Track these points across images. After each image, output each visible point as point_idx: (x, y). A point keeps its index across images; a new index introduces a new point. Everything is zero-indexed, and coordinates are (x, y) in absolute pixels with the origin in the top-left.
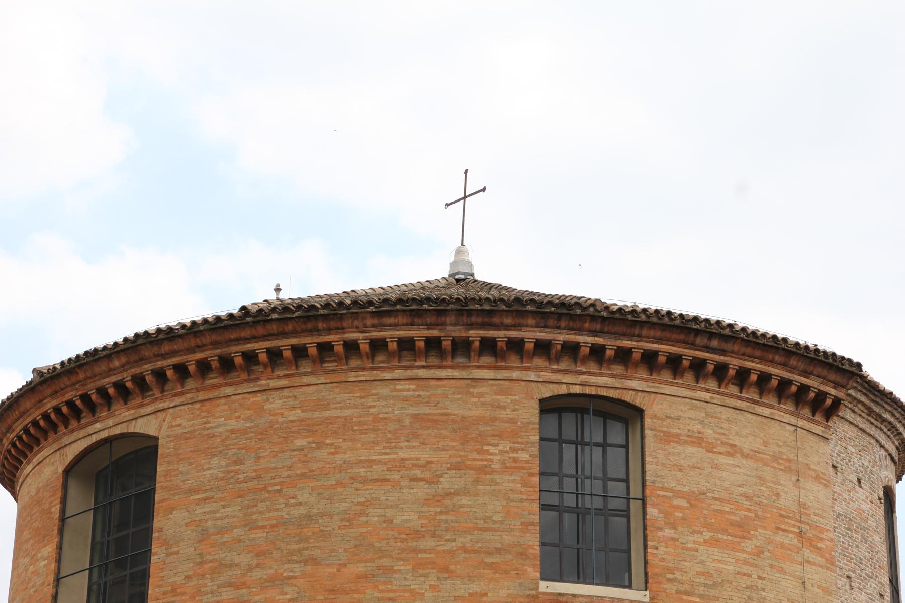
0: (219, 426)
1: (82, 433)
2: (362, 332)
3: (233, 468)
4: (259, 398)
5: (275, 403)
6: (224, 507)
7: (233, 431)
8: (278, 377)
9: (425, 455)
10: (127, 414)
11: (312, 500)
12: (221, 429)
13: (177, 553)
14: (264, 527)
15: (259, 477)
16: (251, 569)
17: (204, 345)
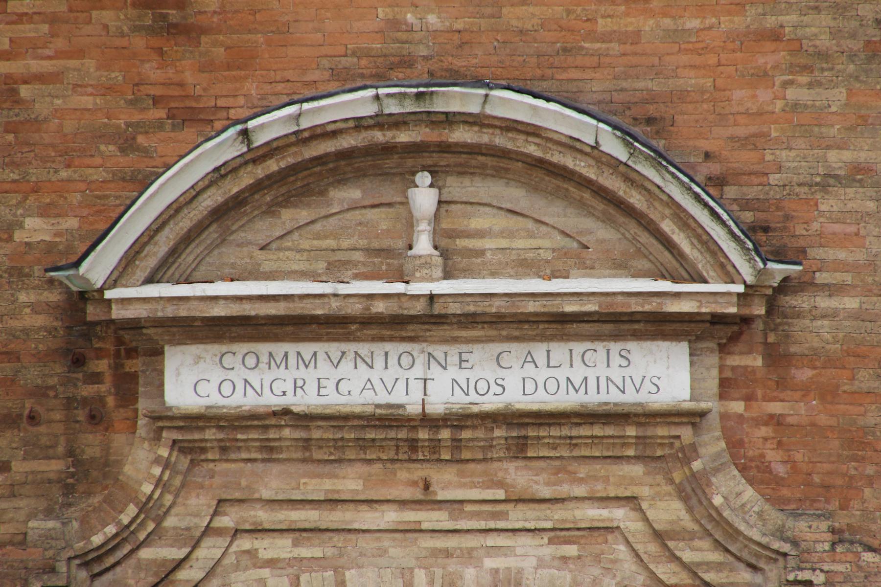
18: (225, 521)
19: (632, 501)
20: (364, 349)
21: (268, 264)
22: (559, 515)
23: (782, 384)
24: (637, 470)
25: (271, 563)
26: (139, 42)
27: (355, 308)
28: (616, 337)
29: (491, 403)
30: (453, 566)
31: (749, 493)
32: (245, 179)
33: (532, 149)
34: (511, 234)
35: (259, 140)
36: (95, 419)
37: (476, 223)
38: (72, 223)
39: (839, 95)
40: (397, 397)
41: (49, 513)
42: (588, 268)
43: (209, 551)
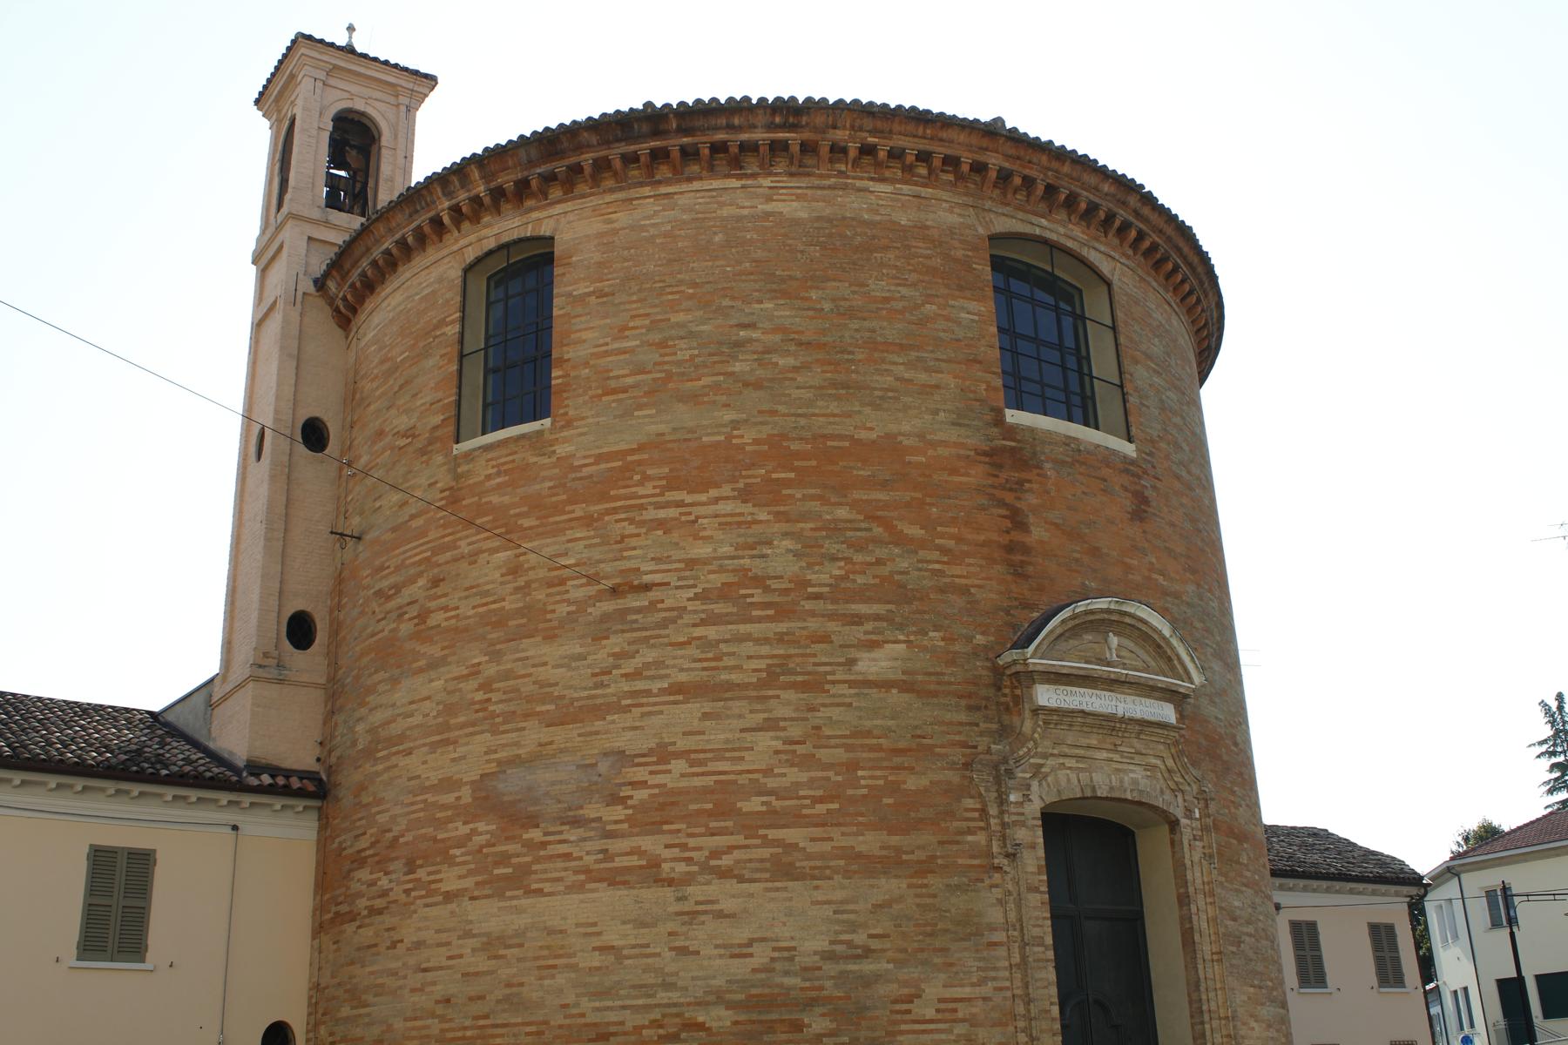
1: (1020, 215)
10: (1077, 232)
17: (1165, 234)
20: (1098, 692)
25: (1070, 768)
26: (1009, 578)
33: (1144, 628)
36: (1007, 709)
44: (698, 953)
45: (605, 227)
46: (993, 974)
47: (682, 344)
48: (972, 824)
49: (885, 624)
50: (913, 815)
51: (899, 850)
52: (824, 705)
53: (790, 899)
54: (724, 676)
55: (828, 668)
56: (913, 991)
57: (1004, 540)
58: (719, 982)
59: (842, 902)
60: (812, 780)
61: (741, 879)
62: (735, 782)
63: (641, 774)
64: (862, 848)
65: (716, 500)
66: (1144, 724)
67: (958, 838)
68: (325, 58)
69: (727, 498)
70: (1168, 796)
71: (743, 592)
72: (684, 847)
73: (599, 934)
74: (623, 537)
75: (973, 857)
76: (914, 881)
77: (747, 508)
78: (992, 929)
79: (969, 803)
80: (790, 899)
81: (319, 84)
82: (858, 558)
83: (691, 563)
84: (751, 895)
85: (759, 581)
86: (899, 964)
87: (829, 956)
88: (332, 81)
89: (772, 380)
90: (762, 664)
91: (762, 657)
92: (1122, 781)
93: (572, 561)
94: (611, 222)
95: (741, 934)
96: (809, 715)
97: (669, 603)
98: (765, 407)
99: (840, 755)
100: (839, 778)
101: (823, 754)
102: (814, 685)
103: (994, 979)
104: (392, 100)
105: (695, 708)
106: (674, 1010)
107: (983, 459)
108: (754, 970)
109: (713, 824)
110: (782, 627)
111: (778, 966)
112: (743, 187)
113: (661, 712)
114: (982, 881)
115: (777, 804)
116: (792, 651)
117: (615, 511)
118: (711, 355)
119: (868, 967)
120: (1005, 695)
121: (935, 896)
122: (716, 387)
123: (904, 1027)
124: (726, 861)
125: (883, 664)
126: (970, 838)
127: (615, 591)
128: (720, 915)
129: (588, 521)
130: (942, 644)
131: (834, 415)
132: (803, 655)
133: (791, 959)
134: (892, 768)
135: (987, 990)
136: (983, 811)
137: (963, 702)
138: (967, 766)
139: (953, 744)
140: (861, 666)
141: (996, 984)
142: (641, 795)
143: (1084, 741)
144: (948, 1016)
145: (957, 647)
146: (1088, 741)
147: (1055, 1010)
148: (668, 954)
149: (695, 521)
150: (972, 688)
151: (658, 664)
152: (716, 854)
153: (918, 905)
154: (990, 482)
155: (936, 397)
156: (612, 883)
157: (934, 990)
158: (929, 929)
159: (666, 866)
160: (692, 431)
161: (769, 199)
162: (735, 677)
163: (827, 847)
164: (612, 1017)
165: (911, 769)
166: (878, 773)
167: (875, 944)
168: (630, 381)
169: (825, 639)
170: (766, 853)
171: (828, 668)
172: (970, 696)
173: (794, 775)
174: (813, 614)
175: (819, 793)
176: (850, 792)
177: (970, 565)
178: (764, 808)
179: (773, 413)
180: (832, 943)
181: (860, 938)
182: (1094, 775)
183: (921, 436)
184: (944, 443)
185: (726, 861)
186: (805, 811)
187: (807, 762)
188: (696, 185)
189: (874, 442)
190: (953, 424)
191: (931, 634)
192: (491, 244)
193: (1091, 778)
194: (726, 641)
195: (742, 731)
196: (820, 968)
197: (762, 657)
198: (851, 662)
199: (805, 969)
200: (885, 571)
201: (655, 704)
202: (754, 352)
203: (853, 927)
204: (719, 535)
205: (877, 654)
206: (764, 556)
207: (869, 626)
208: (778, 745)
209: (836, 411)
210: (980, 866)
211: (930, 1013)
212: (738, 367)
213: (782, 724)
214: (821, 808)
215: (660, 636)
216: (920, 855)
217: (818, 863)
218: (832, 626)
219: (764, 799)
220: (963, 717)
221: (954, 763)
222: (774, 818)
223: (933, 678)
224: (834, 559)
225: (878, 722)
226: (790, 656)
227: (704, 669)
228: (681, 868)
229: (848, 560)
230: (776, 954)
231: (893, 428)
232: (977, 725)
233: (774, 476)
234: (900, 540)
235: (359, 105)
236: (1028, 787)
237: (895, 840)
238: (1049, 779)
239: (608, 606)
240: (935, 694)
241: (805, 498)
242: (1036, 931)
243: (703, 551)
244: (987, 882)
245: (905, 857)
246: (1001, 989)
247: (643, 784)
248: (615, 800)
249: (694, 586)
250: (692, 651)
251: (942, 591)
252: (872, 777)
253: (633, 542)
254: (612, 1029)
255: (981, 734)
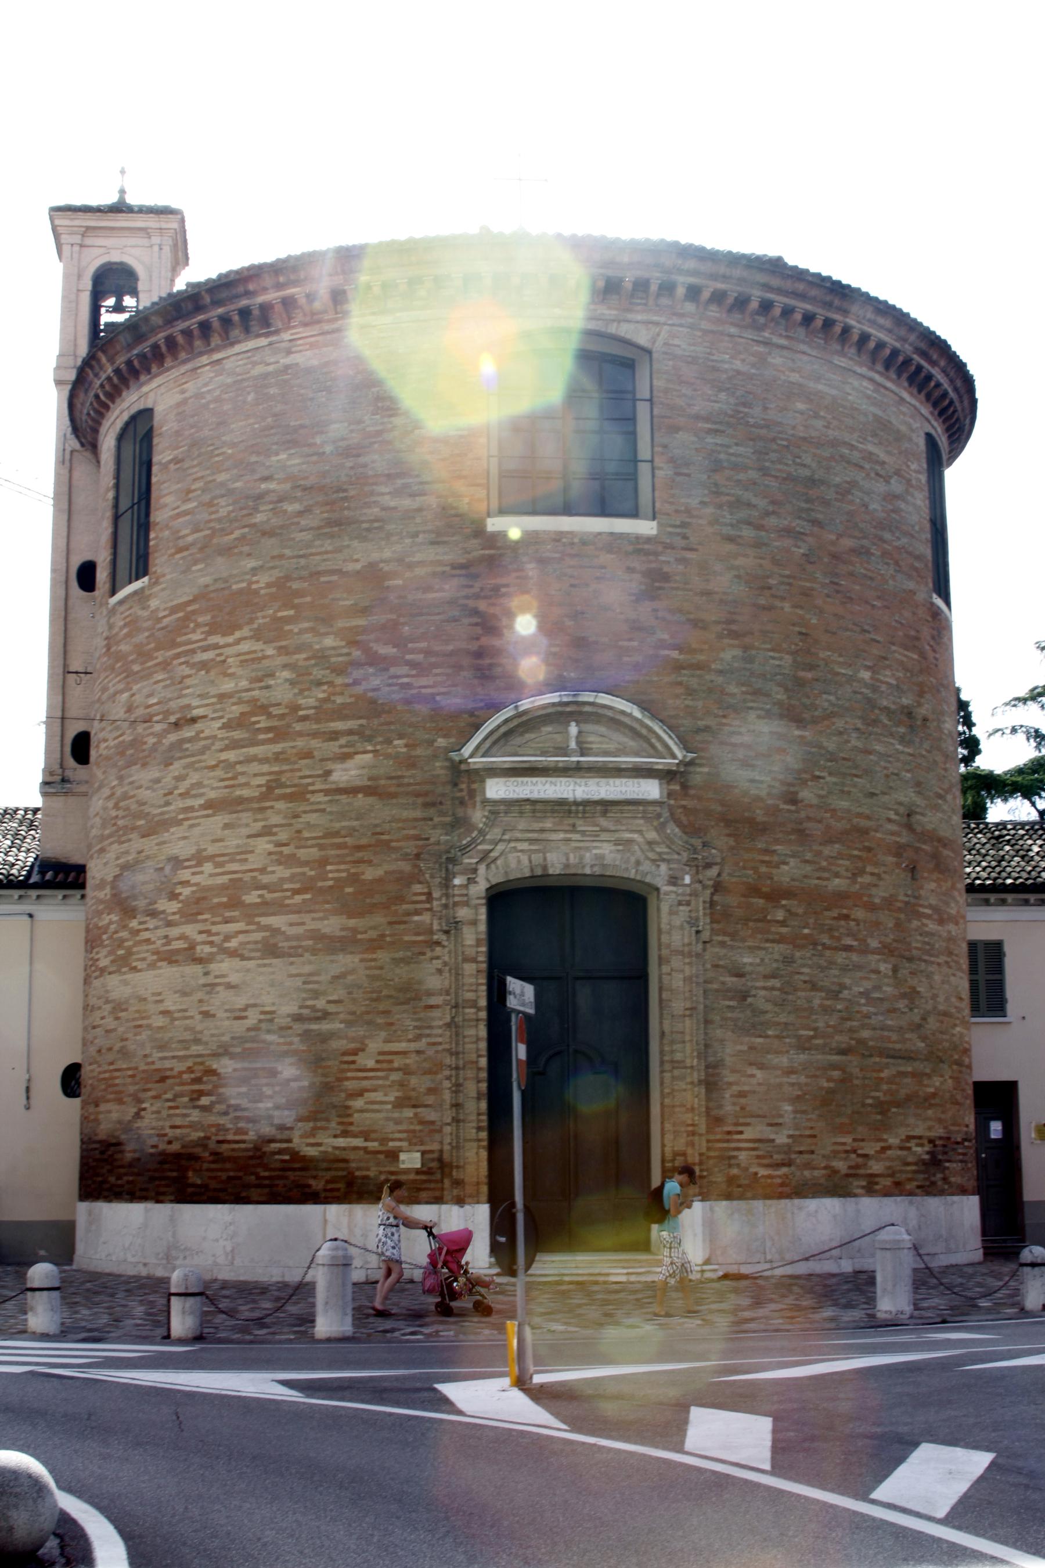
0: (722, 361)
2: (859, 322)
3: (742, 409)
4: (761, 349)
5: (777, 359)
6: (737, 444)
7: (738, 372)
8: (781, 335)
9: (882, 456)
11: (814, 465)
12: (726, 366)
13: (688, 475)
14: (776, 477)
15: (767, 427)
16: (768, 514)
18: (506, 837)
19: (640, 832)
20: (553, 779)
21: (520, 751)
22: (617, 835)
23: (686, 795)
24: (641, 822)
25: (521, 851)
26: (476, 682)
27: (552, 765)
28: (636, 777)
29: (596, 797)
30: (582, 852)
31: (677, 830)
32: (515, 722)
33: (610, 713)
34: (601, 743)
35: (521, 709)
36: (462, 803)
37: (590, 739)
38: (452, 740)
39: (700, 704)
40: (565, 796)
41: (446, 834)
42: (627, 755)
43: (500, 847)
44: (214, 1016)
45: (179, 398)
46: (428, 1031)
47: (222, 502)
48: (418, 906)
49: (356, 738)
50: (368, 901)
51: (355, 931)
52: (305, 812)
53: (273, 973)
54: (238, 793)
55: (309, 780)
56: (358, 1045)
57: (474, 646)
58: (226, 1038)
59: (310, 974)
60: (293, 876)
61: (243, 958)
62: (240, 879)
63: (185, 875)
64: (326, 930)
65: (238, 642)
66: (606, 806)
67: (406, 919)
68: (77, 223)
69: (245, 638)
70: (647, 866)
71: (254, 719)
72: (208, 932)
73: (161, 1001)
74: (184, 677)
75: (418, 934)
76: (366, 956)
77: (258, 646)
78: (430, 994)
79: (418, 888)
80: (273, 973)
81: (76, 248)
82: (339, 681)
83: (222, 697)
84: (248, 970)
85: (264, 709)
86: (349, 1024)
87: (298, 1018)
88: (88, 241)
89: (282, 527)
90: (261, 780)
91: (263, 774)
92: (581, 858)
93: (155, 701)
94: (183, 392)
95: (241, 1001)
96: (293, 821)
97: (207, 733)
98: (275, 553)
99: (314, 853)
100: (313, 873)
101: (303, 854)
102: (299, 795)
103: (428, 1036)
104: (145, 242)
105: (221, 819)
106: (199, 1060)
107: (458, 572)
108: (249, 1030)
109: (227, 914)
110: (278, 747)
111: (263, 1026)
112: (270, 344)
113: (199, 824)
114: (424, 954)
115: (269, 896)
116: (285, 767)
117: (178, 656)
118: (241, 509)
119: (325, 1026)
120: (461, 790)
121: (381, 968)
122: (243, 537)
123: (349, 1074)
124: (233, 944)
125: (353, 773)
126: (416, 918)
127: (177, 725)
128: (229, 986)
129: (165, 665)
130: (404, 750)
131: (327, 552)
132: (292, 771)
133: (271, 1020)
134: (354, 862)
135: (422, 1044)
136: (429, 894)
137: (420, 800)
138: (418, 856)
139: (408, 838)
140: (335, 777)
141: (429, 1040)
142: (186, 891)
143: (537, 826)
144: (385, 1066)
145: (419, 752)
146: (541, 825)
147: (483, 1062)
148: (198, 1017)
149: (224, 661)
150: (427, 787)
151: (199, 785)
152: (227, 938)
153: (368, 976)
154: (463, 594)
155: (418, 520)
156: (171, 962)
157: (375, 1045)
158: (374, 995)
159: (199, 948)
160: (226, 581)
161: (289, 352)
162: (245, 793)
163: (300, 930)
164: (167, 1064)
165: (370, 862)
166: (343, 867)
167: (332, 1008)
168: (190, 539)
169: (308, 755)
170: (258, 936)
171: (309, 780)
172: (426, 794)
173: (282, 872)
174: (300, 734)
175: (297, 886)
176: (320, 884)
177: (436, 675)
178: (258, 900)
179: (281, 557)
180: (301, 1007)
181: (320, 1003)
182: (548, 855)
183: (400, 561)
184: (421, 563)
185: (233, 944)
186: (288, 902)
187: (290, 860)
188: (238, 348)
189: (358, 572)
190: (433, 543)
191: (396, 742)
192: (125, 417)
193: (545, 859)
194: (240, 763)
195: (249, 837)
196: (290, 1028)
197: (263, 774)
198: (328, 773)
199: (281, 1028)
200: (359, 690)
201: (197, 817)
202: (271, 503)
203: (316, 994)
204: (240, 671)
205: (350, 764)
206: (268, 687)
207: (343, 741)
208: (270, 847)
209: (330, 548)
210: (425, 942)
211: (371, 1064)
212: (259, 518)
213: (275, 830)
214: (298, 899)
215: (200, 761)
216: (373, 934)
217: (294, 943)
218: (315, 743)
219: (260, 892)
220: (418, 814)
221: (407, 854)
222: (266, 907)
223: (394, 782)
224: (319, 684)
225: (344, 824)
226: (281, 772)
227: (226, 787)
228: (207, 949)
229: (330, 683)
230: (262, 1017)
231: (375, 556)
232: (431, 819)
233: (280, 614)
234: (374, 660)
235: (115, 257)
236: (475, 871)
237: (352, 923)
238: (499, 862)
239: (173, 737)
240: (393, 795)
241: (301, 632)
242: (470, 996)
243: (228, 686)
244: (429, 954)
245: (359, 936)
246: (434, 1044)
247: (186, 883)
248: (173, 896)
249: (221, 717)
250: (219, 773)
251: (408, 702)
252: (338, 871)
253: (188, 682)
254: (168, 1073)
255: (434, 827)
